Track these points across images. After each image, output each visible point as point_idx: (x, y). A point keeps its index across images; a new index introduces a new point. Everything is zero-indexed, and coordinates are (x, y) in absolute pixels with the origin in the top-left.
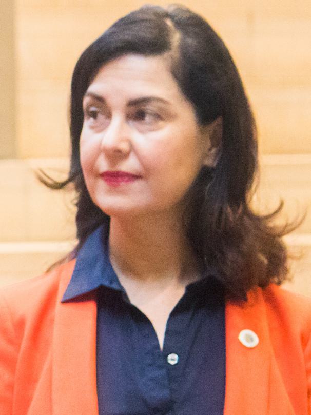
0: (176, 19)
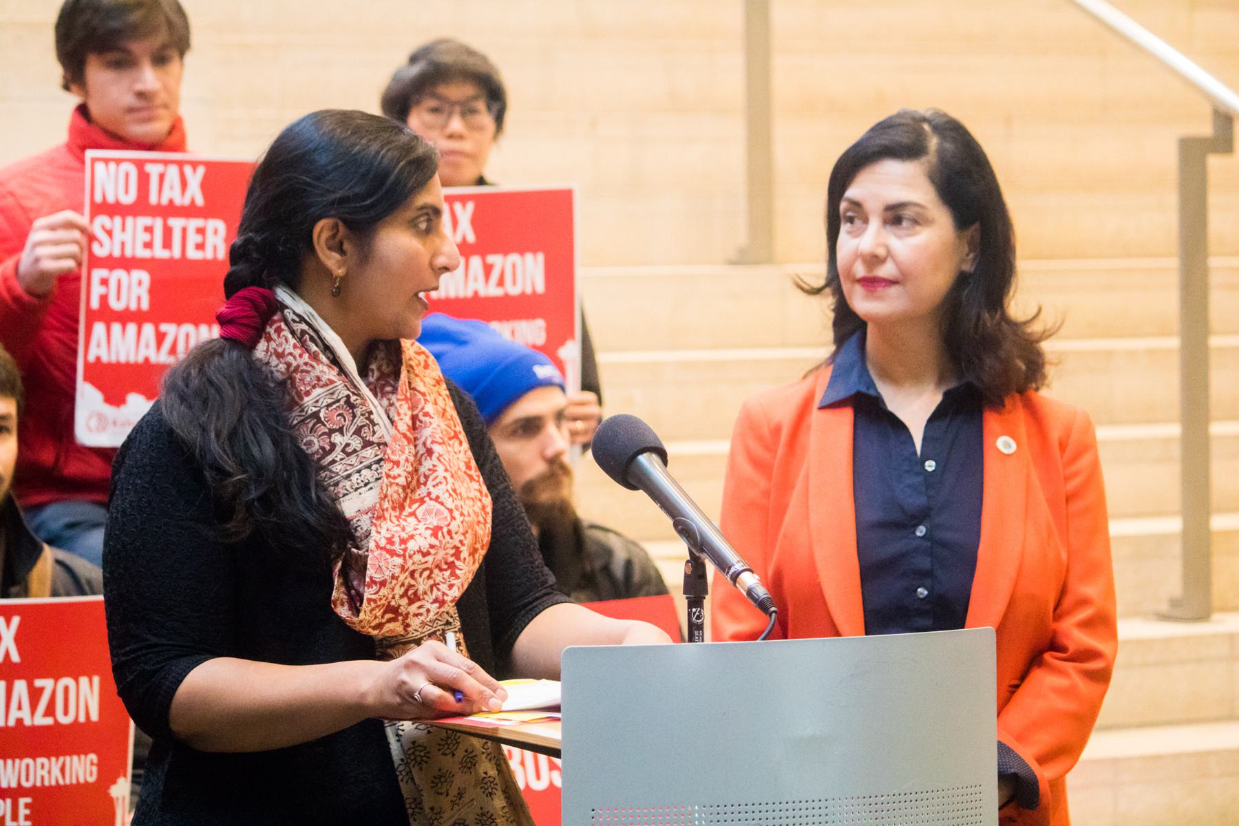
0: (933, 123)
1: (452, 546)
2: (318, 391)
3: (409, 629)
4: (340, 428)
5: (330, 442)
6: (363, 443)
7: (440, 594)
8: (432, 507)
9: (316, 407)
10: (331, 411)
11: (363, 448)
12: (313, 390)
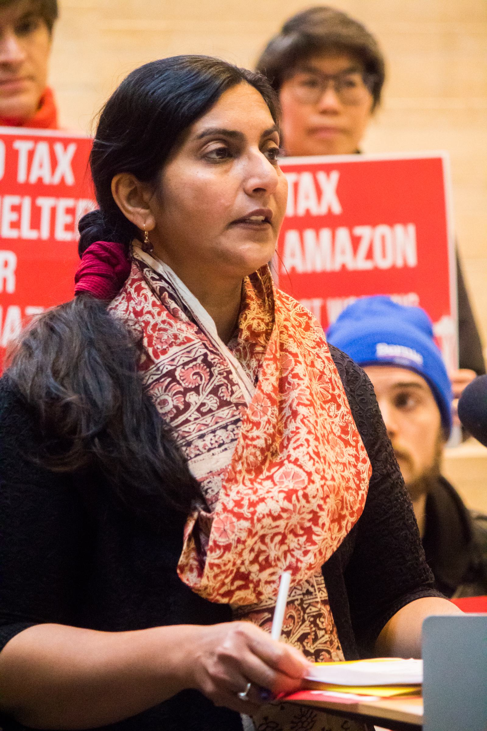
1: (309, 510)
3: (262, 597)
4: (196, 387)
5: (185, 401)
6: (220, 403)
7: (294, 560)
8: (290, 470)
9: (172, 365)
10: (188, 369)
11: (219, 407)
12: (170, 348)
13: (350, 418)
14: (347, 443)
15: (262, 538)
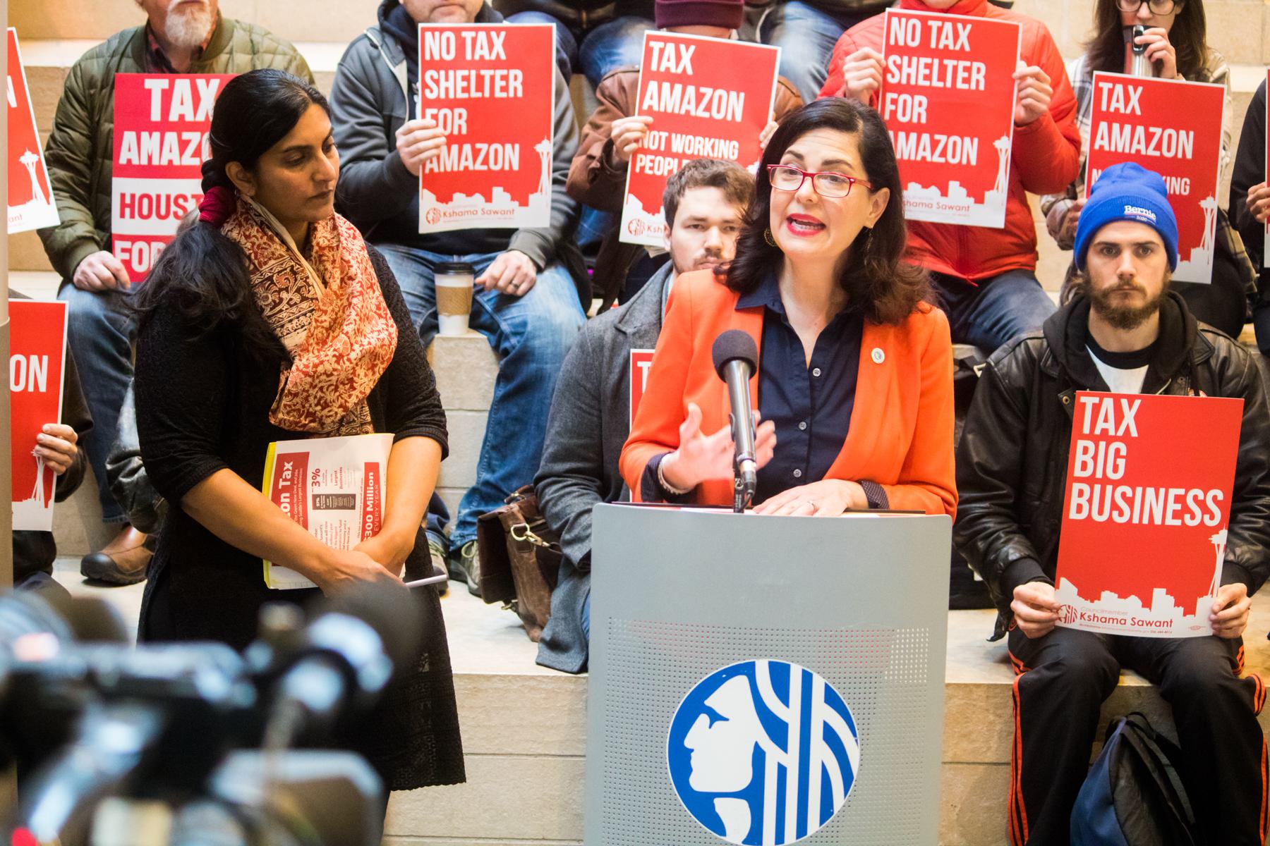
2: (272, 262)
13: (381, 299)
14: (380, 316)
15: (321, 388)
